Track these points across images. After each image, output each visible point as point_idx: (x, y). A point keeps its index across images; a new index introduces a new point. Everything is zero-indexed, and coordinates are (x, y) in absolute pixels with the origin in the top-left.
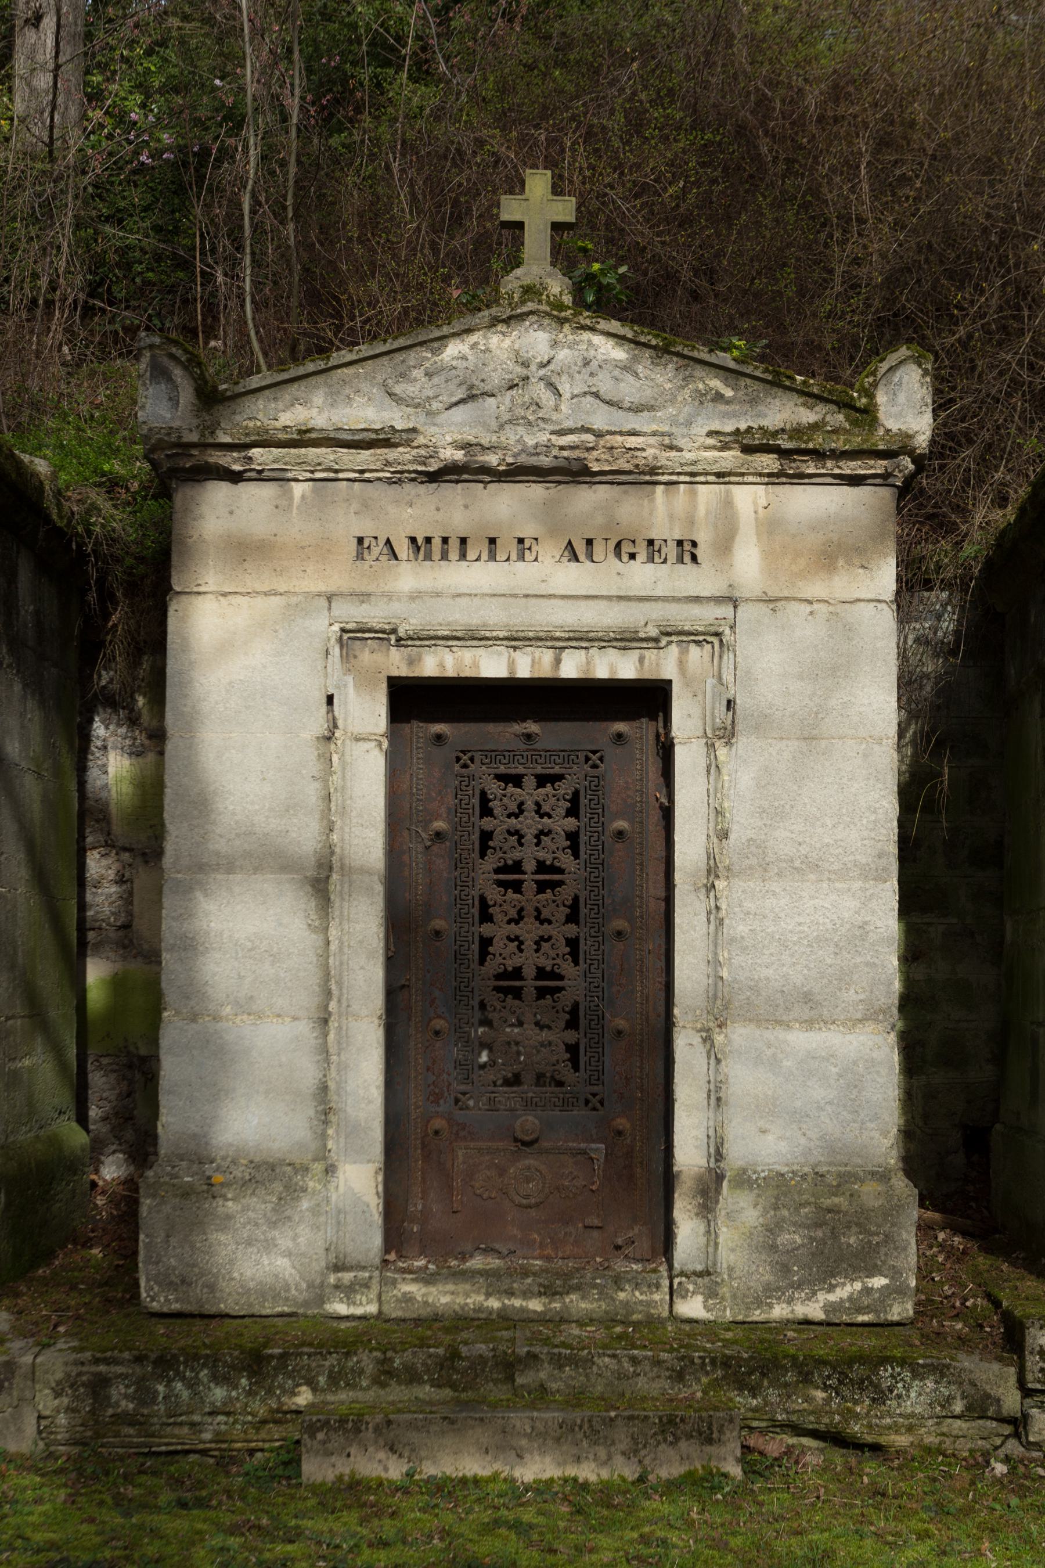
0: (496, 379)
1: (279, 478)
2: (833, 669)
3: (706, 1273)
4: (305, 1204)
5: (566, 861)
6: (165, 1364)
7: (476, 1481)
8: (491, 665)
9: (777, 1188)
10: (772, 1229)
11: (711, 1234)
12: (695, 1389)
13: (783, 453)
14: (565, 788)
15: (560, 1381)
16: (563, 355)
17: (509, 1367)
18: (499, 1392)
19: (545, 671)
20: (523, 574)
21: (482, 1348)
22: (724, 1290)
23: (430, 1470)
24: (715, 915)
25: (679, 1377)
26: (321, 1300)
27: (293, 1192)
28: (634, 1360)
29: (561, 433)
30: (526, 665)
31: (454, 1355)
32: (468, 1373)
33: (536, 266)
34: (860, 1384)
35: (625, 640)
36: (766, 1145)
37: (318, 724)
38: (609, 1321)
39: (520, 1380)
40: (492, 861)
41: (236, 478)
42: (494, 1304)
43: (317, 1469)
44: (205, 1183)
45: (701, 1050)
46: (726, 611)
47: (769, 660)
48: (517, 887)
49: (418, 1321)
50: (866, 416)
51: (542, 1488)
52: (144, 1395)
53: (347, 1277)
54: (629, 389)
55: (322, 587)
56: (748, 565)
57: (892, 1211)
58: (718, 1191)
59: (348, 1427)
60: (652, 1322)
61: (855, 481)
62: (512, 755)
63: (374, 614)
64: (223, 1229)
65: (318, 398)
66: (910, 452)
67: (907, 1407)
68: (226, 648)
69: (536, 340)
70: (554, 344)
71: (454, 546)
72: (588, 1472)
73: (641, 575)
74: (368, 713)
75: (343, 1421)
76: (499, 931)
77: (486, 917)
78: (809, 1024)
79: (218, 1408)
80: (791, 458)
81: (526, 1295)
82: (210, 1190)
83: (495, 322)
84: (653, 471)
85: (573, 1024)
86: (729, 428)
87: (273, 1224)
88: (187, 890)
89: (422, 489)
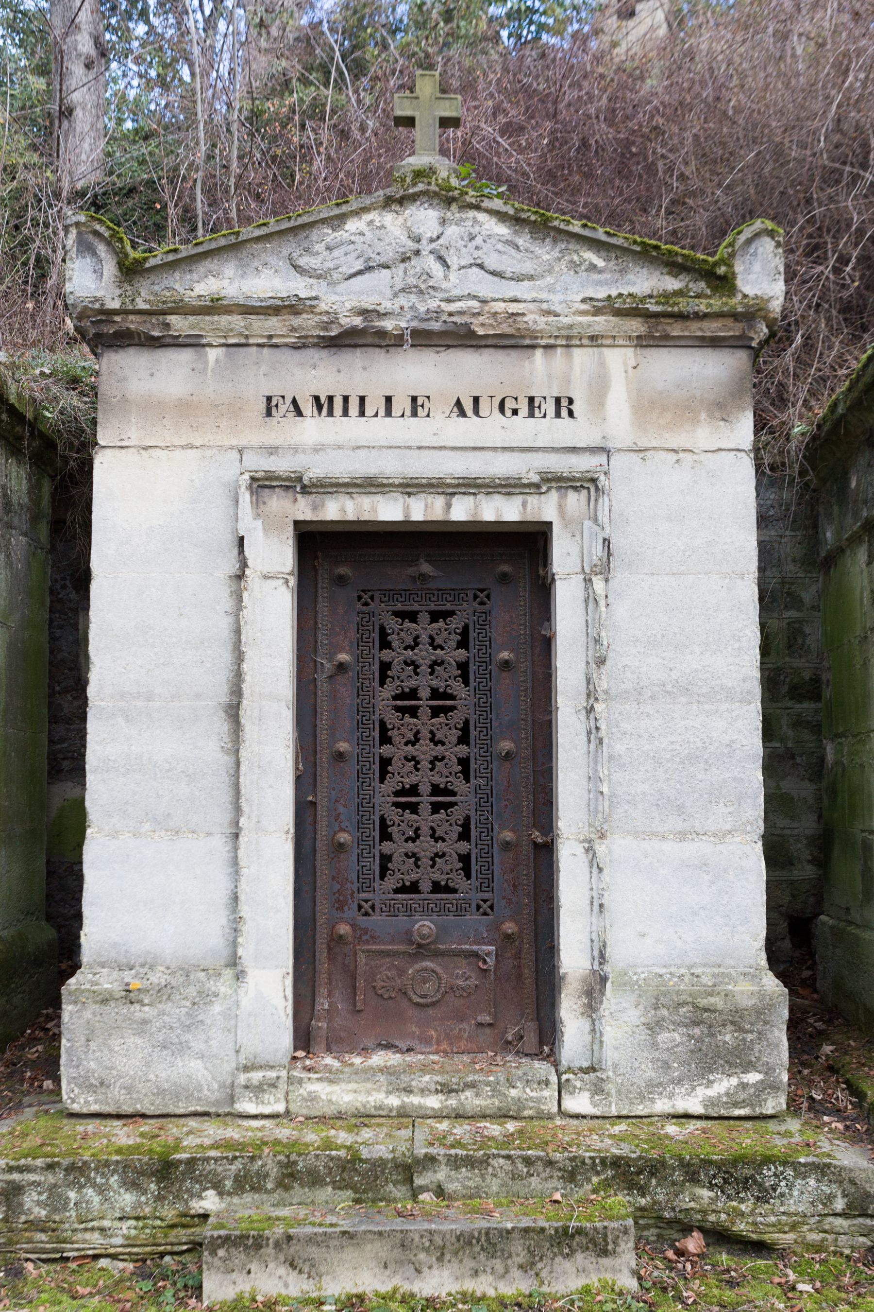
1: (194, 343)
3: (592, 1069)
8: (389, 510)
13: (648, 315)
14: (456, 623)
16: (452, 231)
22: (610, 1087)
29: (449, 301)
30: (420, 510)
35: (508, 487)
37: (231, 566)
39: (418, 1181)
45: (583, 859)
46: (603, 459)
50: (723, 283)
52: (56, 1202)
53: (256, 1076)
54: (510, 263)
56: (618, 420)
57: (762, 1012)
58: (602, 992)
59: (249, 1244)
63: (282, 465)
70: (443, 222)
72: (484, 1285)
73: (522, 430)
74: (275, 556)
80: (657, 326)
86: (601, 294)
89: (324, 353)
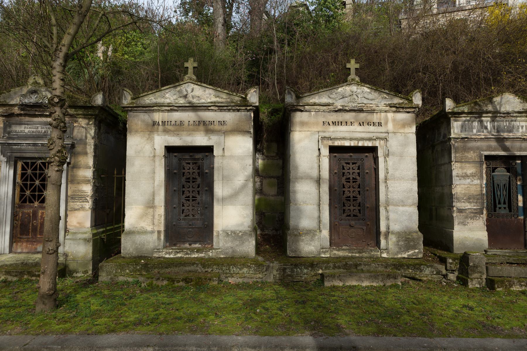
0: (347, 95)
1: (309, 111)
2: (405, 145)
3: (386, 249)
4: (316, 237)
5: (358, 177)
6: (296, 266)
7: (355, 286)
8: (347, 144)
9: (399, 234)
10: (398, 241)
11: (387, 242)
12: (389, 270)
13: (397, 107)
14: (357, 165)
15: (365, 268)
16: (359, 90)
17: (356, 266)
18: (355, 270)
19: (356, 145)
20: (351, 128)
21: (351, 262)
22: (390, 252)
23: (347, 284)
24: (387, 187)
25: (386, 267)
26: (320, 254)
27: (314, 235)
28: (378, 265)
29: (359, 104)
30: (353, 144)
31: (347, 264)
32: (350, 267)
33: (353, 75)
34: (418, 269)
35: (370, 139)
36: (395, 227)
37: (317, 153)
38: (370, 258)
39: (358, 268)
40: (345, 177)
41: (302, 111)
42: (350, 255)
43: (327, 284)
44: (298, 234)
45: (384, 211)
46: (387, 134)
47: (394, 143)
48: (349, 182)
49: (337, 258)
50: (411, 101)
51: (367, 287)
52: (292, 271)
53: (324, 250)
54: (370, 96)
55: (317, 130)
56: (390, 127)
57: (418, 239)
58: (388, 235)
59: (333, 277)
60: (377, 258)
61: (408, 112)
62: (348, 159)
63: (327, 135)
64: (302, 242)
65: (317, 98)
66: (418, 107)
67: (426, 273)
68: (300, 141)
69: (354, 88)
70: (357, 89)
71: (340, 123)
72: (375, 284)
73: (372, 128)
74: (325, 152)
75: (332, 275)
76: (346, 190)
77: (344, 187)
78: (403, 206)
79: (306, 274)
80: (398, 108)
81: (355, 253)
82: (300, 235)
83: (347, 85)
84: (374, 110)
85: (359, 206)
86: (388, 103)
87: (311, 241)
88: (294, 182)
89: (334, 113)
